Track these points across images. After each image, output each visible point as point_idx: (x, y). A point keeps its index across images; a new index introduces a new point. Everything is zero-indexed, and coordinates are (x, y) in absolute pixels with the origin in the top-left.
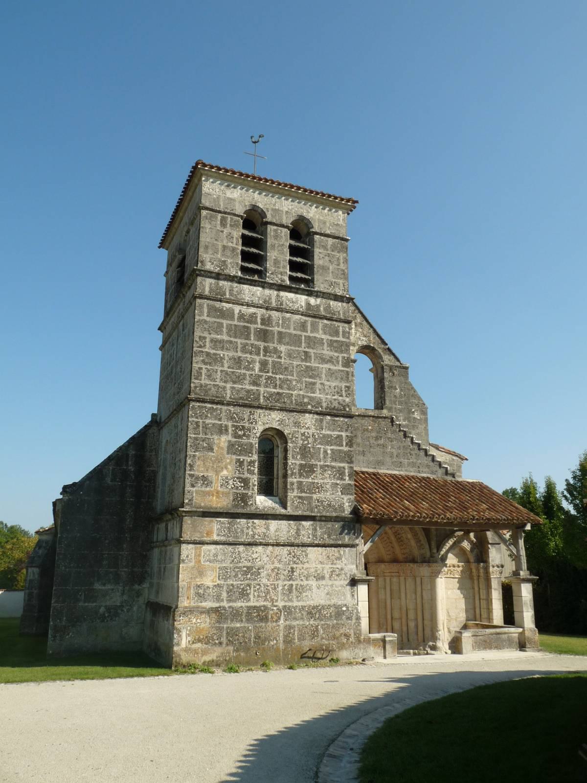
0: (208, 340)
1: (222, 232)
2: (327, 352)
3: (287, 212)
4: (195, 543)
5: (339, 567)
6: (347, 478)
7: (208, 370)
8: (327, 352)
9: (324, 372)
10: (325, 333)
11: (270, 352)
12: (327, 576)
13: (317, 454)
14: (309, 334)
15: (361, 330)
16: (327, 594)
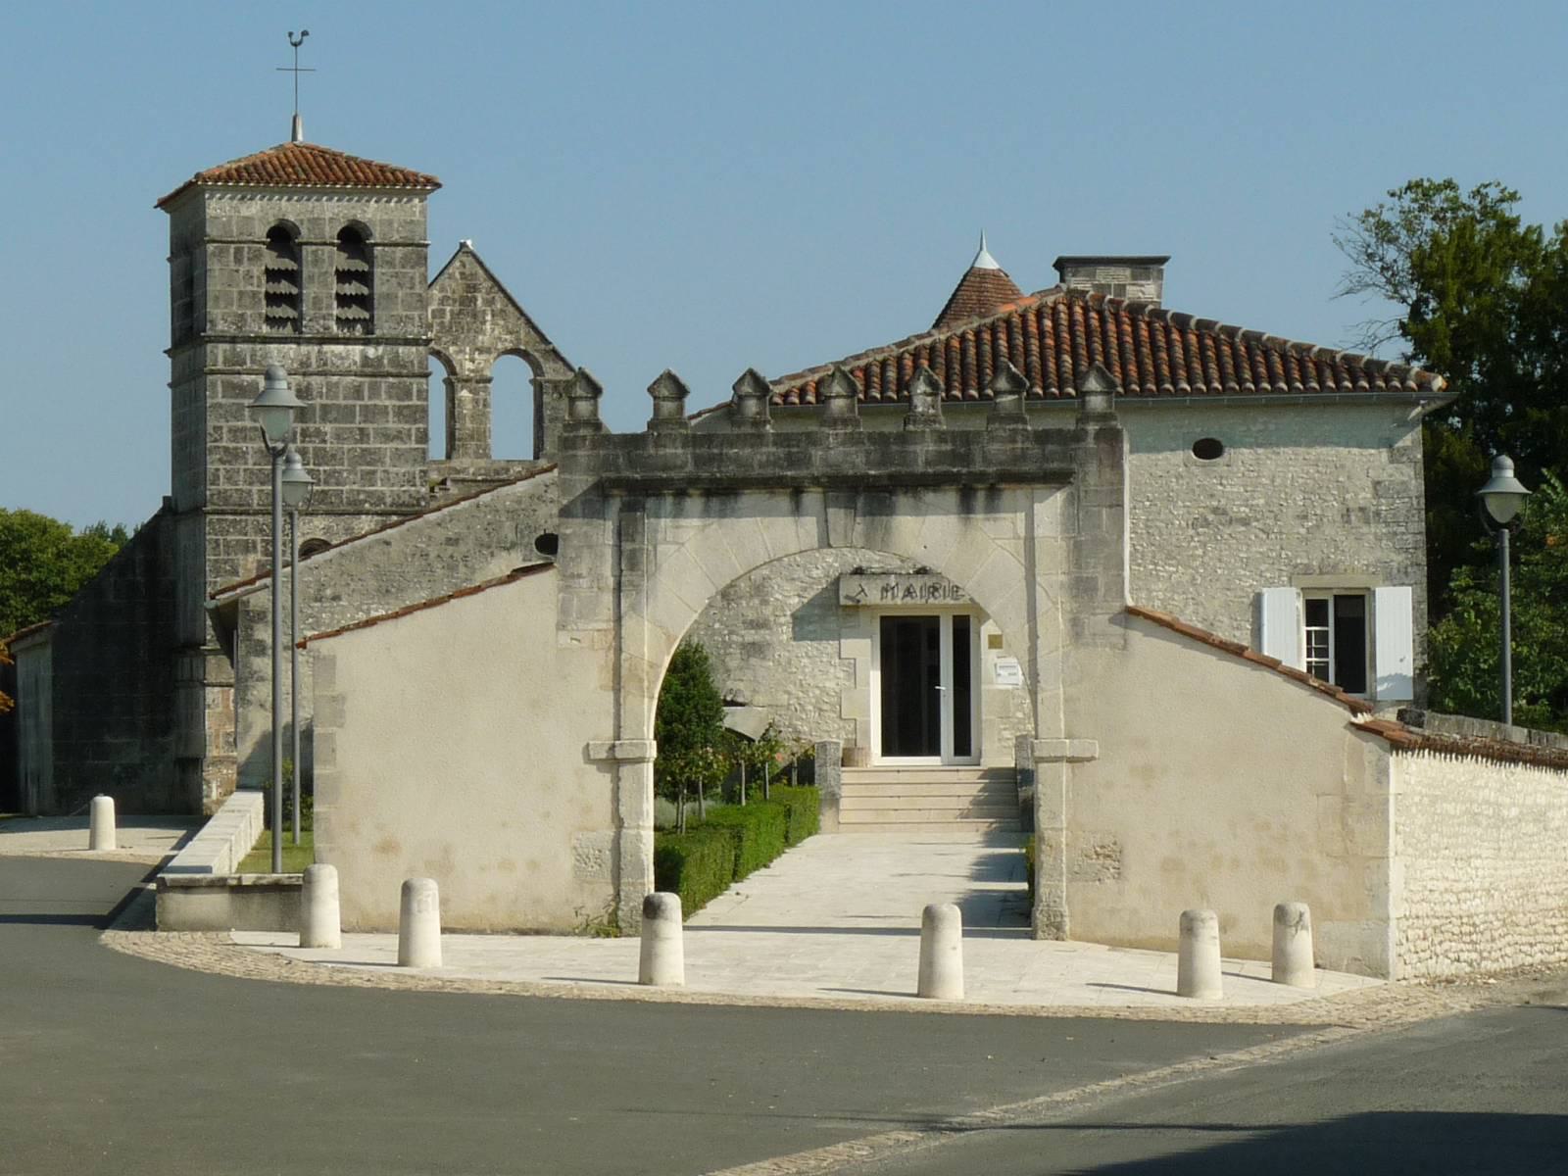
0: (225, 430)
1: (237, 271)
2: (392, 425)
3: (331, 219)
4: (221, 685)
7: (227, 471)
8: (392, 425)
9: (388, 454)
10: (390, 397)
11: (310, 436)
14: (366, 402)
15: (502, 322)
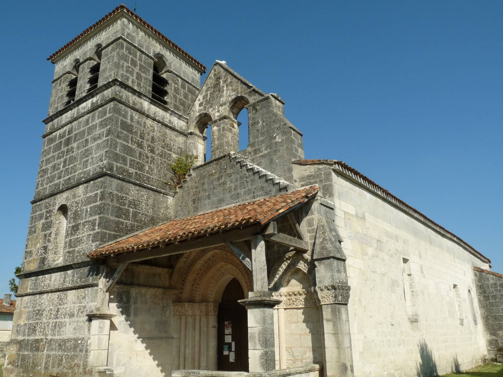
5: (83, 305)
6: (97, 227)
12: (76, 314)
13: (82, 215)
15: (230, 88)
16: (74, 329)
